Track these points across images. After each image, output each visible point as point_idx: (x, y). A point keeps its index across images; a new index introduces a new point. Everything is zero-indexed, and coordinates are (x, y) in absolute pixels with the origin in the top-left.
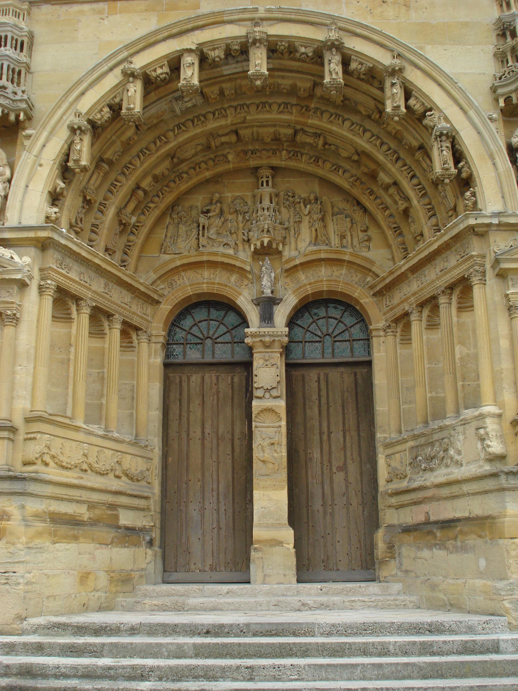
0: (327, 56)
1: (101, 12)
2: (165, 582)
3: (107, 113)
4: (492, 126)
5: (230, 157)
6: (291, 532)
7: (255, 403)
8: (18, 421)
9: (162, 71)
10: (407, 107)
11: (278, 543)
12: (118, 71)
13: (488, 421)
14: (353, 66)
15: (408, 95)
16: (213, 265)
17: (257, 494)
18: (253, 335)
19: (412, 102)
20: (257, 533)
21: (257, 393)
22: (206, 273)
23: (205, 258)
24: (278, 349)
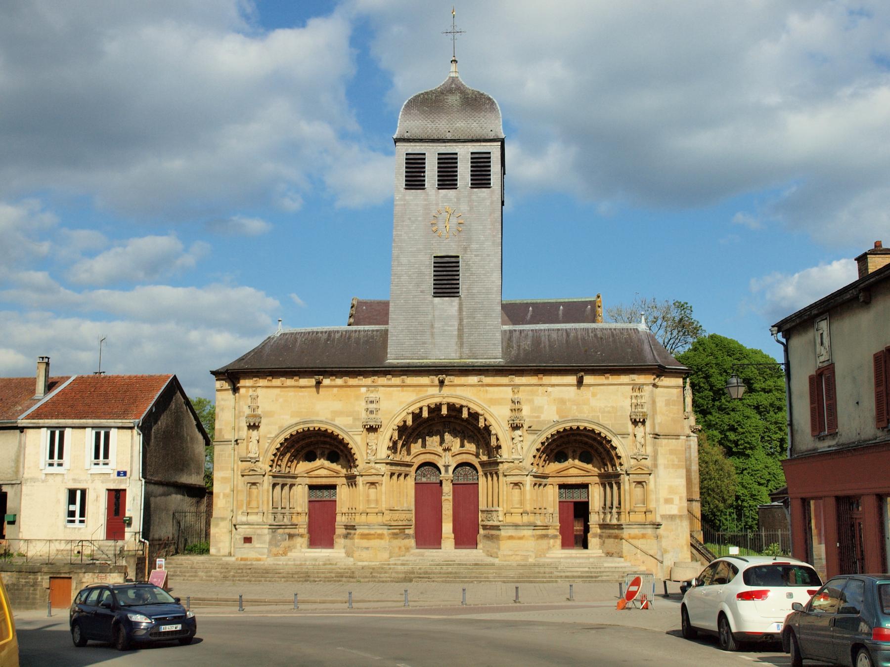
0: (464, 409)
1: (399, 391)
2: (417, 548)
3: (402, 423)
4: (507, 432)
5: (436, 419)
6: (453, 535)
7: (443, 497)
8: (384, 510)
9: (417, 411)
10: (485, 424)
11: (449, 538)
12: (405, 411)
13: (500, 512)
14: (470, 411)
15: (485, 420)
16: (429, 453)
17: (443, 524)
18: (443, 477)
19: (486, 422)
20: (443, 536)
21: (444, 494)
22: (428, 454)
23: (428, 451)
24: (450, 481)
